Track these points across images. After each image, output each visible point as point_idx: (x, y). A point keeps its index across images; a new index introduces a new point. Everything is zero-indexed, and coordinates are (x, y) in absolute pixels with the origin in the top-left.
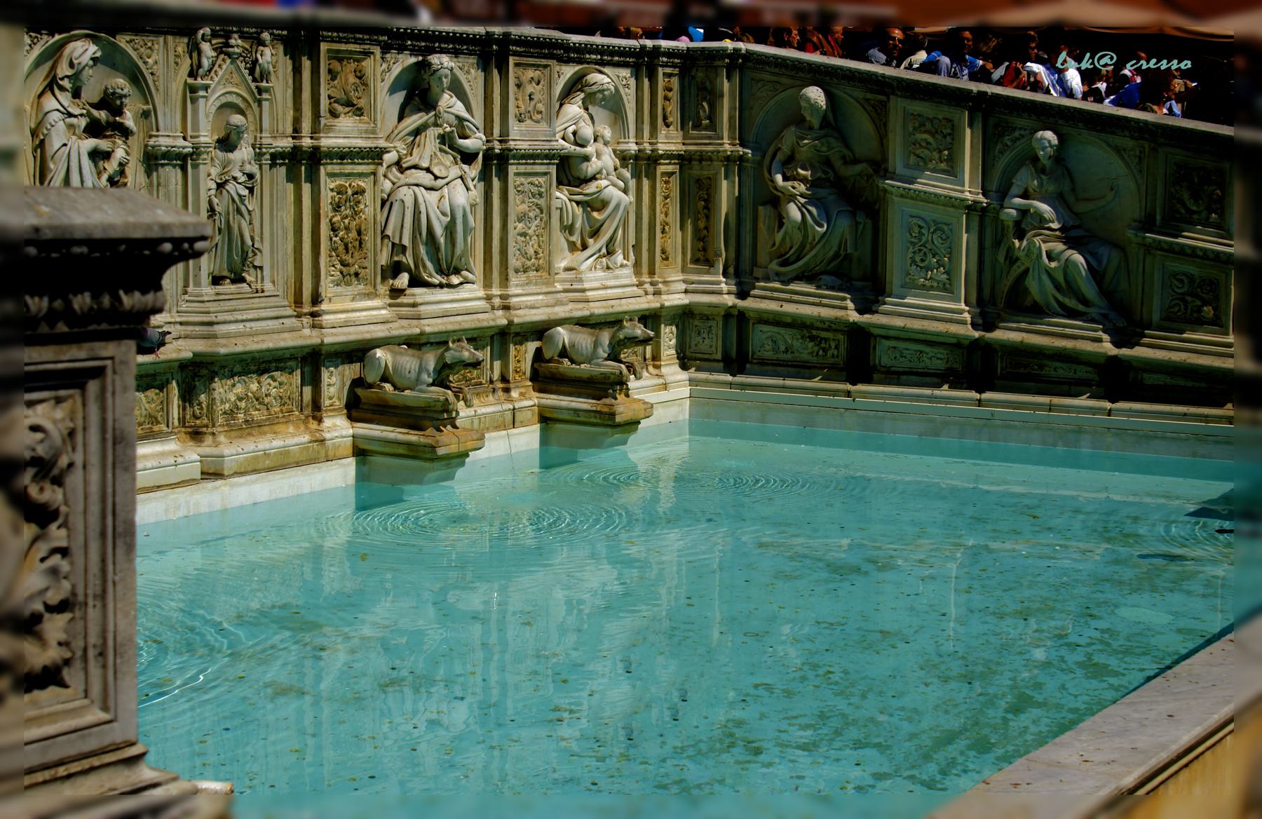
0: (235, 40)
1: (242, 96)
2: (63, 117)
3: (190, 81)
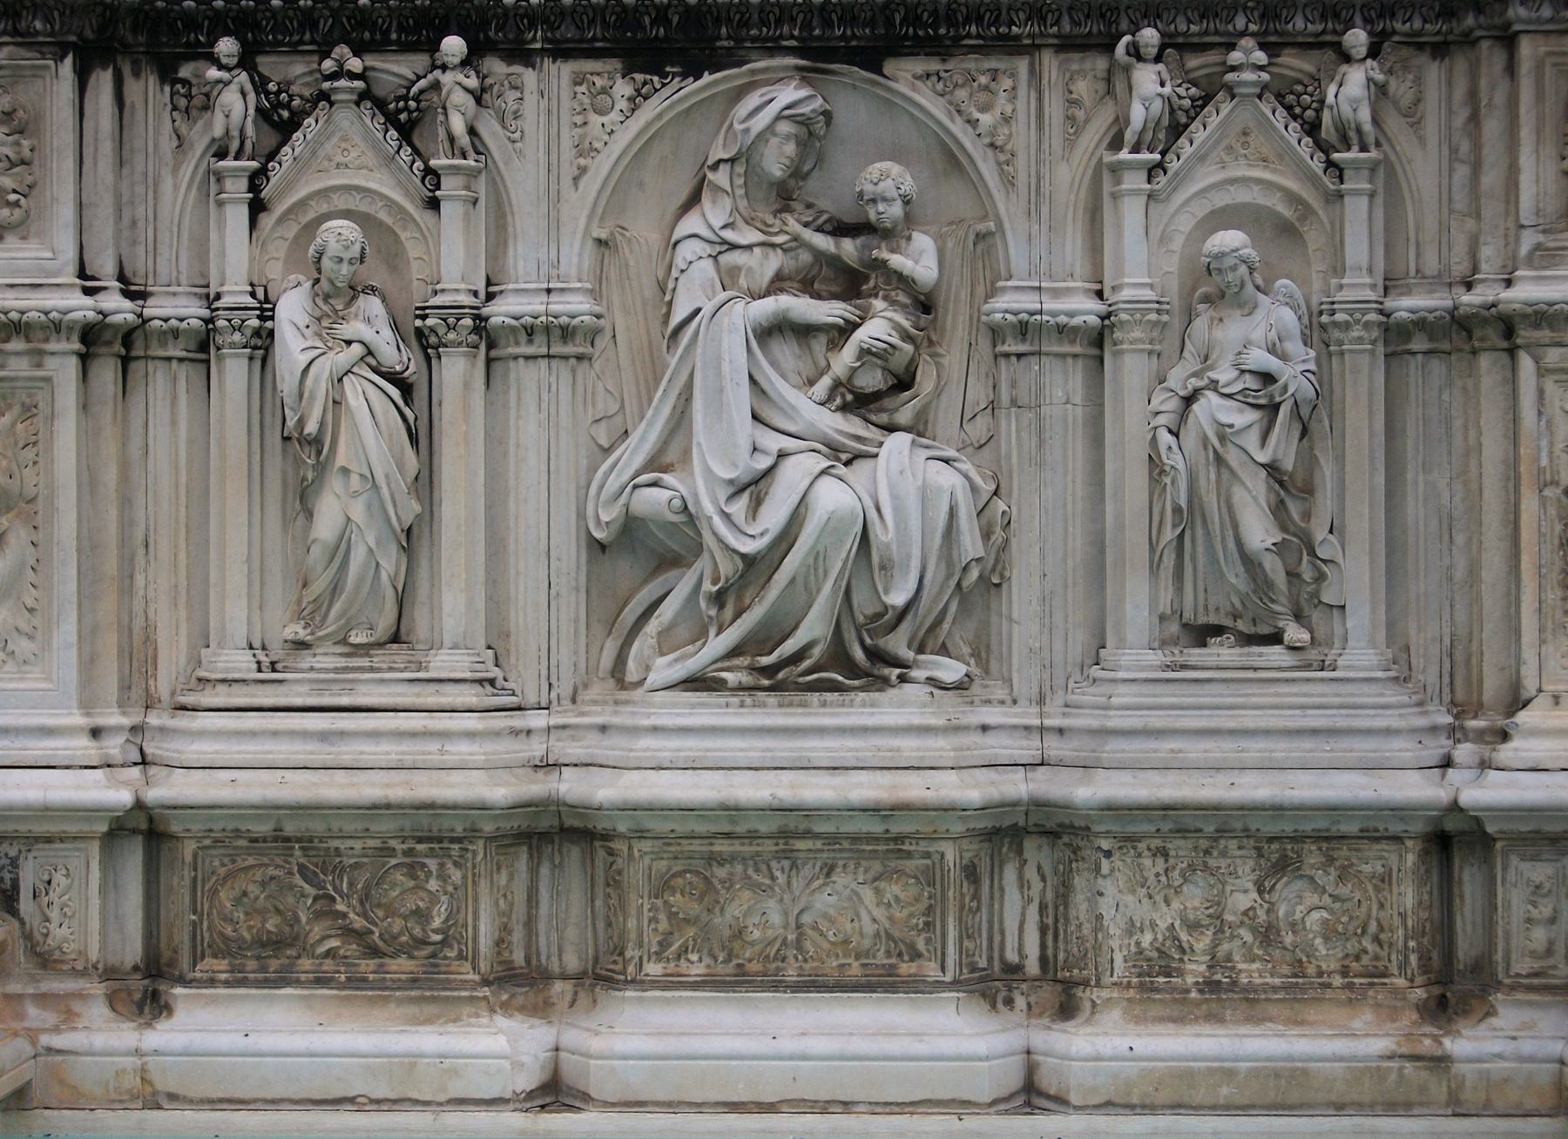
0: (1248, 53)
1: (1259, 181)
2: (709, 249)
3: (1109, 158)
